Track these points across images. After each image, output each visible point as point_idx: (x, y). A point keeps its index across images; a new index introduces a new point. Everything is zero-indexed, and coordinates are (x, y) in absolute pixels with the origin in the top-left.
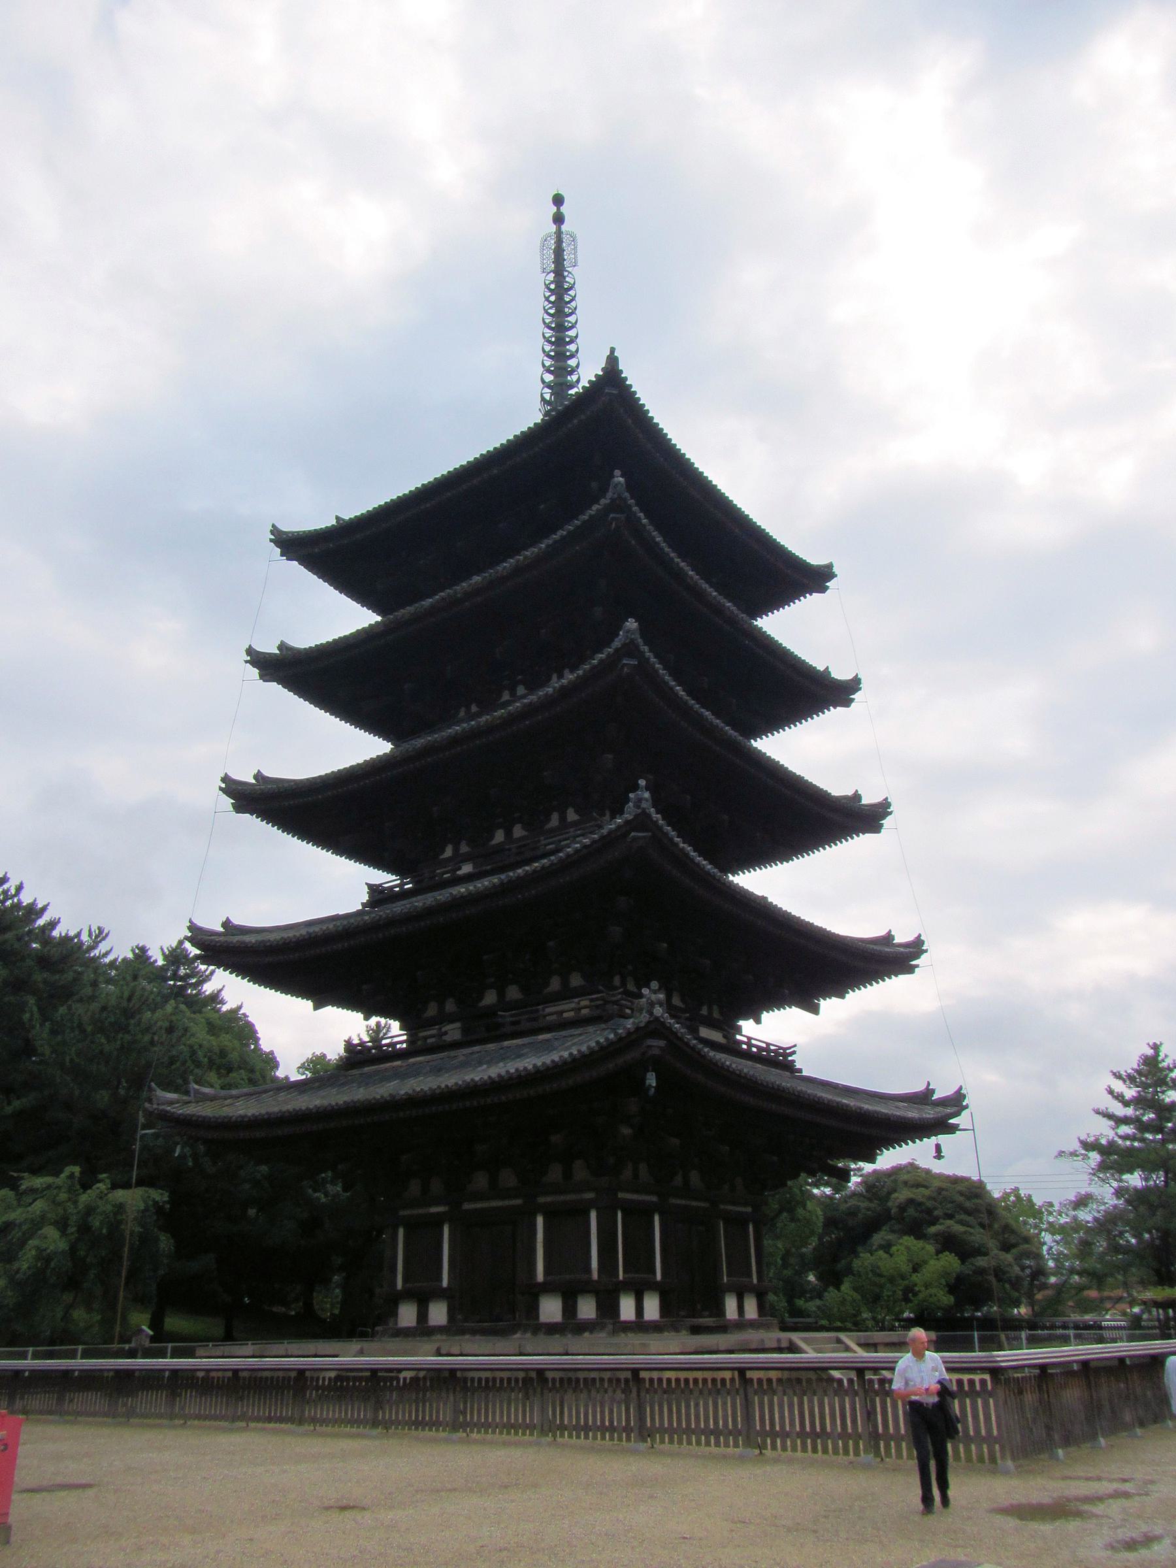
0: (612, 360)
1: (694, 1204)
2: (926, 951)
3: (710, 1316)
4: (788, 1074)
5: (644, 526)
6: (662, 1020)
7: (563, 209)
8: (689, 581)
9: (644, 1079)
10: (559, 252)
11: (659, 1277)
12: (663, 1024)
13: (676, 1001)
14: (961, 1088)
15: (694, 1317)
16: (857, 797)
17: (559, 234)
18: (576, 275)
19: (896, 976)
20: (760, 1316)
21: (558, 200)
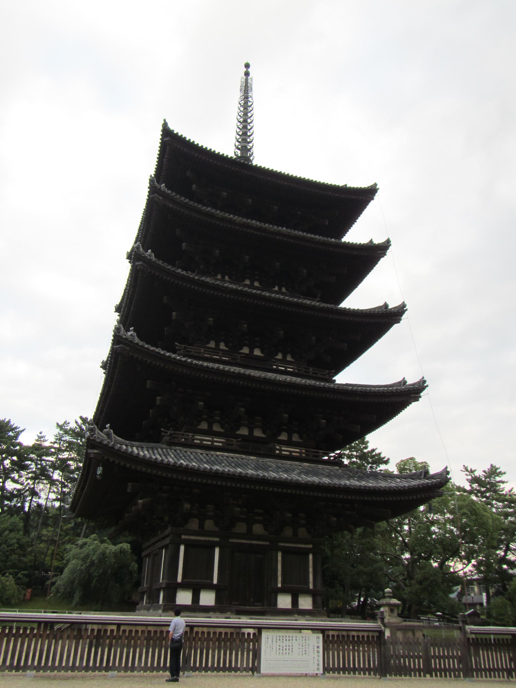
0: (165, 125)
1: (254, 542)
2: (427, 386)
3: (263, 605)
4: (337, 468)
5: (173, 196)
6: (92, 438)
7: (249, 70)
8: (218, 216)
9: (96, 471)
10: (246, 89)
11: (215, 581)
12: (94, 440)
13: (258, 433)
14: (446, 468)
15: (246, 606)
16: (386, 305)
17: (247, 80)
18: (255, 95)
19: (411, 404)
20: (313, 607)
21: (247, 66)
